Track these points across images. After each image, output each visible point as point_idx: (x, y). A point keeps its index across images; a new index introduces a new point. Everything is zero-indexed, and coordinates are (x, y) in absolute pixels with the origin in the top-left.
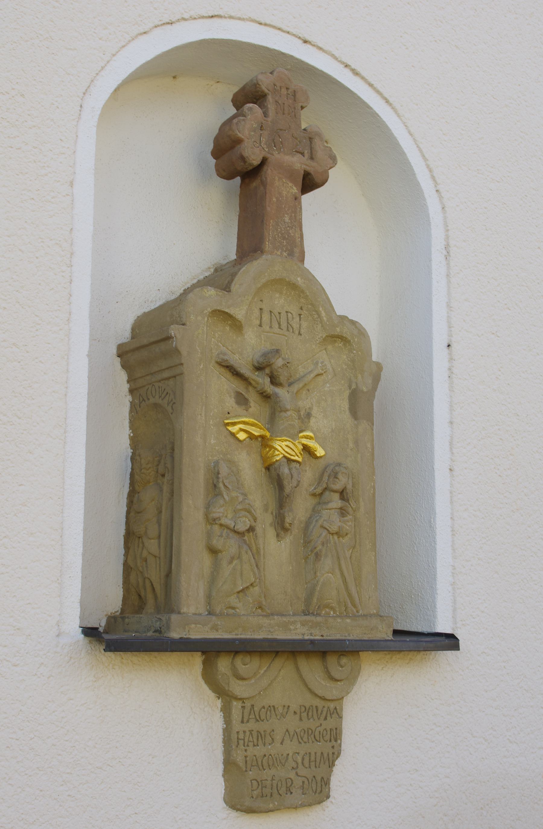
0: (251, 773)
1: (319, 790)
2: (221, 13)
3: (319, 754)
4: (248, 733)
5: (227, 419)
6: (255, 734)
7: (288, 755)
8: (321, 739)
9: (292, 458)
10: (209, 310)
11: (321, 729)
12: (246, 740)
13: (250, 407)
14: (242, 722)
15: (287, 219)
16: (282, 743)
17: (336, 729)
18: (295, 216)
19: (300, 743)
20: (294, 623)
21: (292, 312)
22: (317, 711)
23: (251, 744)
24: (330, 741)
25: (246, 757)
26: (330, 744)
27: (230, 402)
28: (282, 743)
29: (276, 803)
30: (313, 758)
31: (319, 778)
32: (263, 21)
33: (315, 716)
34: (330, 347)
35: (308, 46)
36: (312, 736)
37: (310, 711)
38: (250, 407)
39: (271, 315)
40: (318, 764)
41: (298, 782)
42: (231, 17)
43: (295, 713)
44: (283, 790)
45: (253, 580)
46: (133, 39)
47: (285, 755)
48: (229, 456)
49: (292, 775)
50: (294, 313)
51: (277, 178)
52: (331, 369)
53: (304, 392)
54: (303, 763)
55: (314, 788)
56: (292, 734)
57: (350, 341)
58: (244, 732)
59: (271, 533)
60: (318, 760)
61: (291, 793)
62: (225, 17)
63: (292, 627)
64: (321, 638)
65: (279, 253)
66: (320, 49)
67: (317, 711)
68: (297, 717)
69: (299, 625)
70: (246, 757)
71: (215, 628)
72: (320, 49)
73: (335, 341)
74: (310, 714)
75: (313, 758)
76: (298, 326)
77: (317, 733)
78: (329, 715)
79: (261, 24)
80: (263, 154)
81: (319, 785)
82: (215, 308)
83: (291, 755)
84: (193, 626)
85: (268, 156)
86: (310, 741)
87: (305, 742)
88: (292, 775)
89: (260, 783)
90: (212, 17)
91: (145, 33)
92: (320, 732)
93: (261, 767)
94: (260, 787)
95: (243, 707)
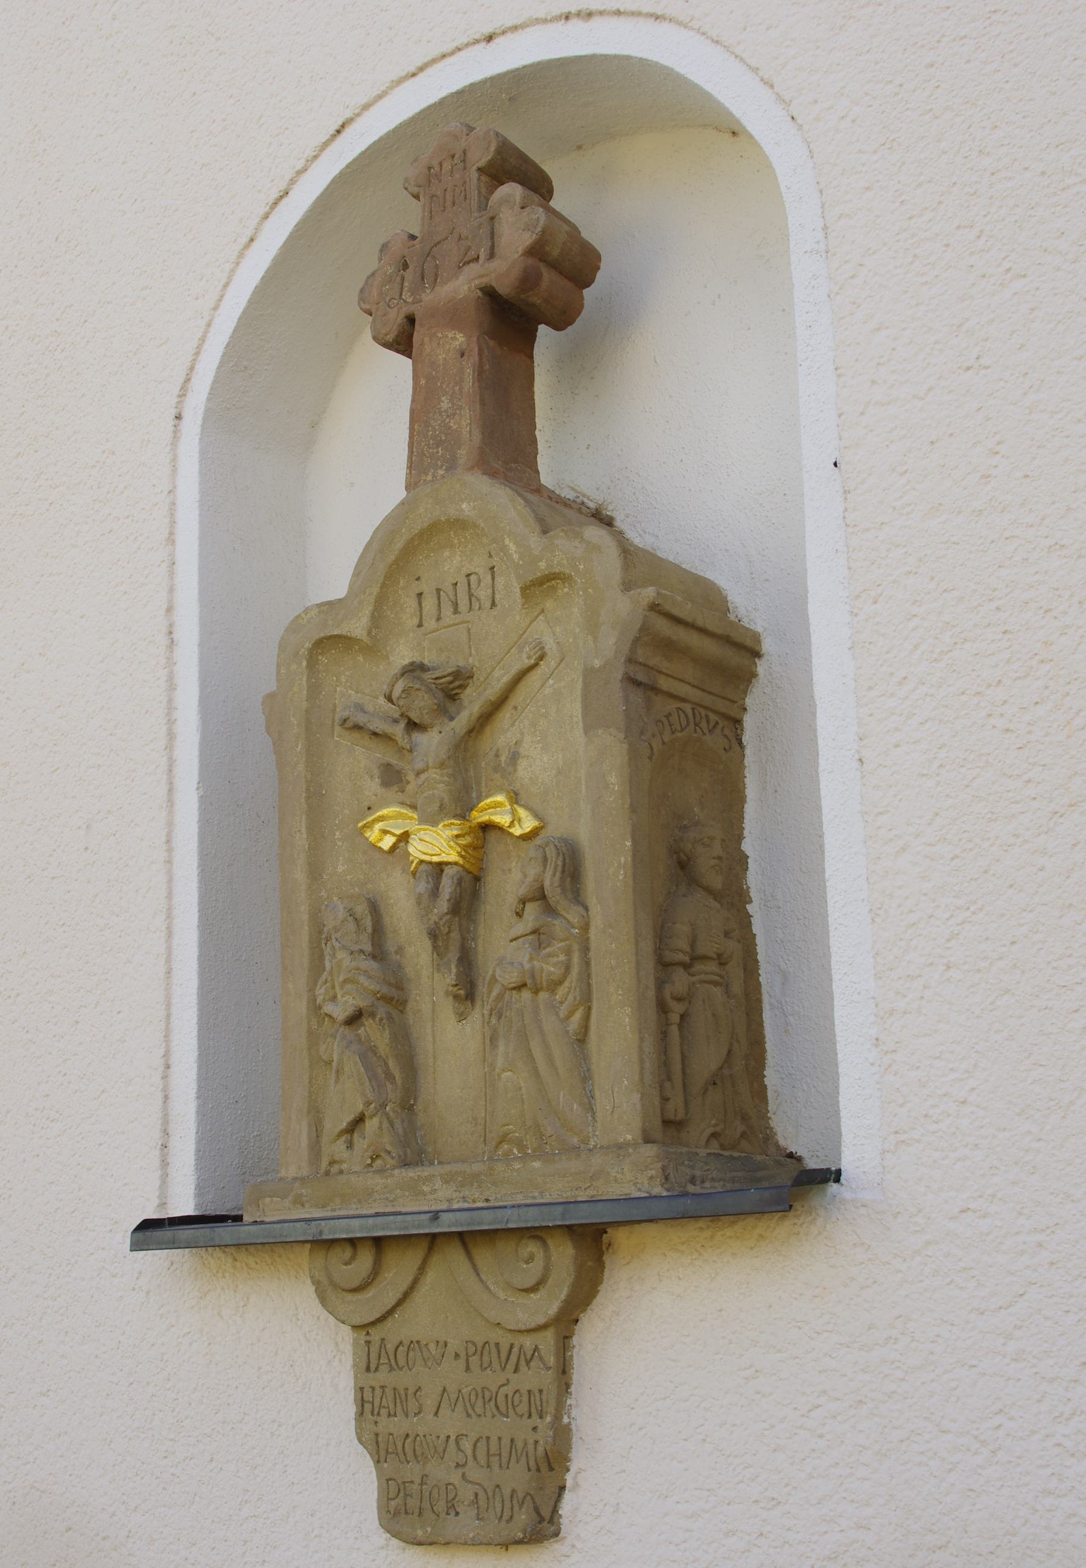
0: (386, 1465)
1: (507, 1514)
2: (348, 114)
3: (506, 1442)
4: (378, 1392)
5: (362, 820)
6: (389, 1392)
7: (448, 1437)
8: (511, 1410)
9: (435, 859)
10: (308, 645)
11: (508, 1390)
12: (377, 1404)
13: (408, 782)
14: (368, 1369)
15: (445, 404)
16: (436, 1414)
17: (541, 1391)
18: (461, 389)
19: (469, 1415)
20: (429, 1179)
21: (477, 570)
22: (499, 1352)
23: (383, 1411)
24: (530, 1416)
25: (377, 1435)
26: (530, 1423)
27: (372, 786)
28: (436, 1414)
29: (429, 1530)
30: (494, 1449)
31: (507, 1492)
32: (413, 69)
33: (496, 1365)
34: (549, 604)
35: (498, 41)
36: (492, 1403)
37: (486, 1352)
38: (408, 782)
39: (439, 598)
40: (504, 1460)
41: (466, 1493)
42: (366, 107)
43: (457, 1355)
44: (441, 1506)
45: (360, 1107)
46: (238, 263)
47: (443, 1437)
48: (369, 886)
49: (455, 1478)
50: (480, 571)
51: (426, 339)
52: (555, 647)
53: (508, 715)
54: (475, 1457)
55: (499, 1510)
56: (454, 1396)
57: (570, 576)
58: (373, 1388)
59: (447, 1009)
60: (505, 1455)
61: (457, 1514)
62: (358, 115)
63: (426, 1188)
64: (485, 1204)
65: (429, 478)
66: (515, 28)
67: (499, 1352)
68: (462, 1361)
69: (438, 1184)
70: (377, 1435)
71: (299, 1202)
72: (515, 28)
73: (554, 589)
74: (486, 1358)
75: (494, 1449)
76: (490, 591)
77: (501, 1399)
78: (523, 1362)
79: (414, 75)
80: (405, 310)
81: (507, 1504)
82: (317, 637)
83: (453, 1438)
84: (268, 1200)
85: (411, 309)
86: (489, 1414)
87: (479, 1416)
88: (455, 1478)
89: (402, 1487)
90: (338, 132)
91: (252, 240)
92: (507, 1396)
93: (402, 1457)
94: (402, 1494)
95: (368, 1343)
